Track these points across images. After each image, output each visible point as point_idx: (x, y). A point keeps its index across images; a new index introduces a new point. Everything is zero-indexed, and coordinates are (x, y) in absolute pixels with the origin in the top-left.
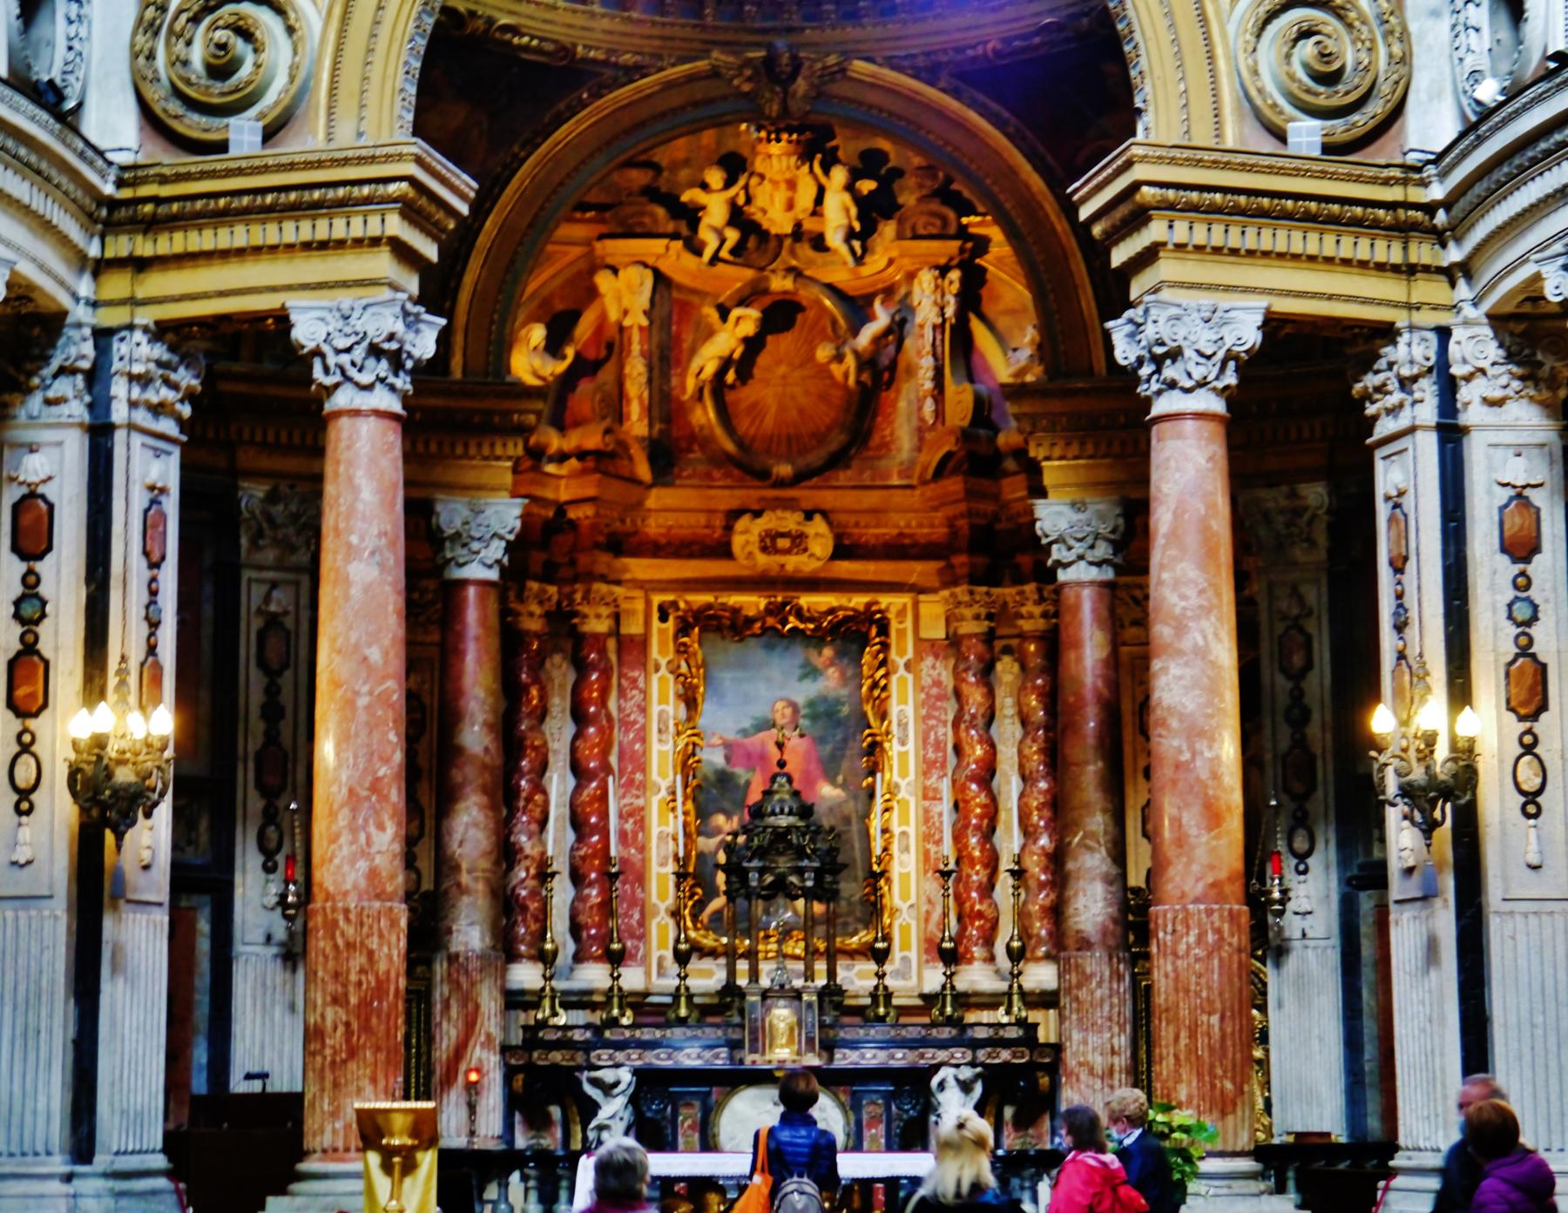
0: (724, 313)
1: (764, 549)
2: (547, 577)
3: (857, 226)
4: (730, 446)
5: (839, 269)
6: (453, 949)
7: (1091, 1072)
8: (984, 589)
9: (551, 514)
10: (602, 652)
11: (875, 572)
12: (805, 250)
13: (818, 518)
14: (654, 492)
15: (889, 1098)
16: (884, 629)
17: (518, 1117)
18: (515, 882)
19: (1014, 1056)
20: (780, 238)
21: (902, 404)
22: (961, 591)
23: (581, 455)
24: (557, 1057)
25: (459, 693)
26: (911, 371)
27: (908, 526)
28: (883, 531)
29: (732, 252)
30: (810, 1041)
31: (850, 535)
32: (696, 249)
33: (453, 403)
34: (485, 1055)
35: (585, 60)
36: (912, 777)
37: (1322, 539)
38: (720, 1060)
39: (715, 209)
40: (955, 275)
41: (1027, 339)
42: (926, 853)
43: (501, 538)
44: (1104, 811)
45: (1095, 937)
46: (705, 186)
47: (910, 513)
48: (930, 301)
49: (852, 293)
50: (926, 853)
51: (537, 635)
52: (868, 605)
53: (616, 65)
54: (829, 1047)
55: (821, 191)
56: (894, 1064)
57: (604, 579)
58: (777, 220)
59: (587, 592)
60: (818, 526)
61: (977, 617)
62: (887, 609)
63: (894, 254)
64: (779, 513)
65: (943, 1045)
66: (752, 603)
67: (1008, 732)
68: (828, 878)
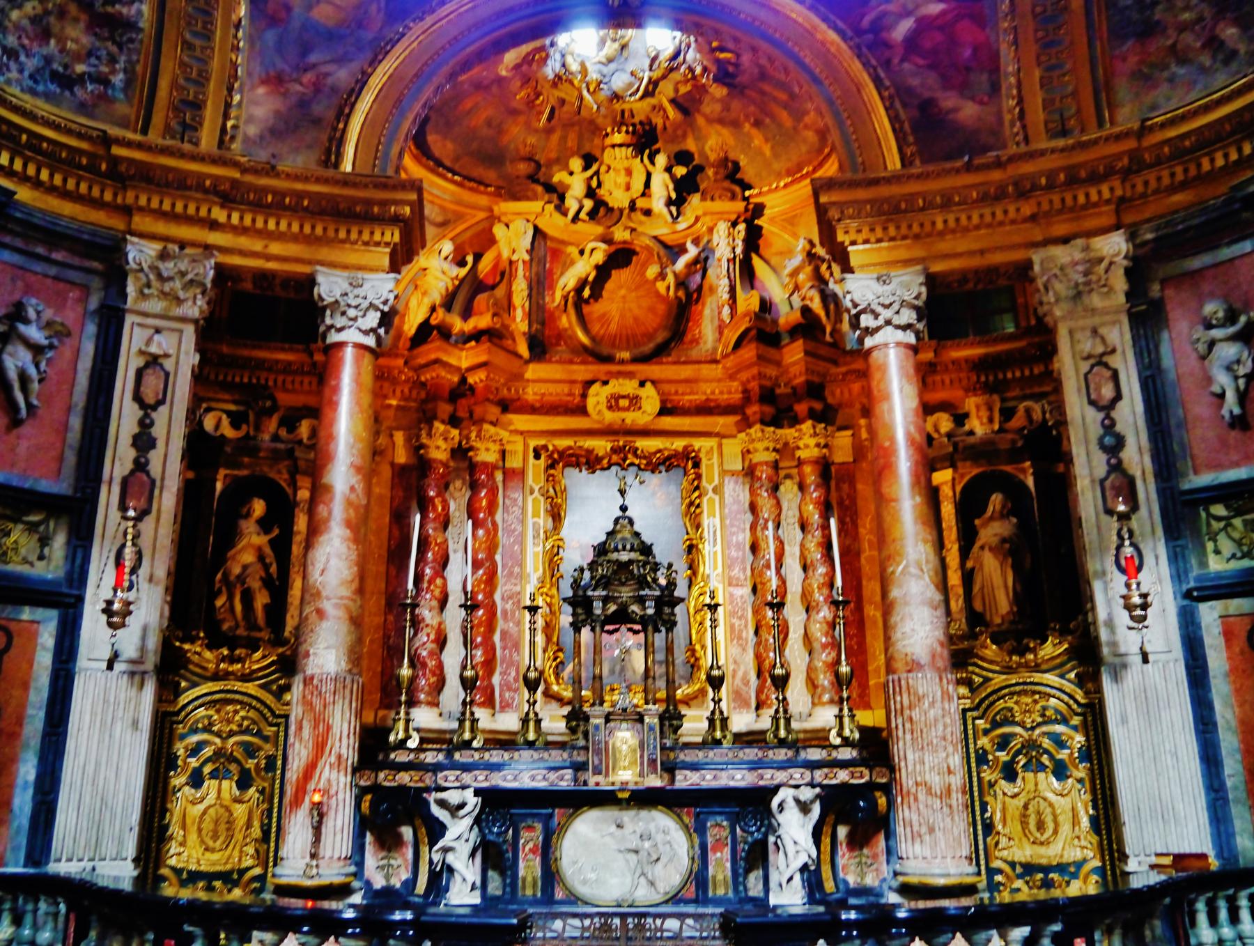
0: (582, 252)
1: (610, 408)
2: (454, 421)
3: (674, 196)
5: (661, 226)
6: (309, 672)
7: (929, 791)
8: (772, 429)
9: (456, 379)
10: (491, 476)
11: (690, 425)
12: (638, 216)
13: (648, 385)
14: (531, 366)
15: (734, 820)
16: (697, 465)
17: (369, 838)
18: (417, 645)
19: (852, 775)
20: (621, 211)
21: (707, 312)
22: (755, 431)
23: (477, 336)
24: (405, 778)
25: (331, 437)
26: (712, 290)
27: (713, 393)
28: (696, 397)
29: (588, 214)
30: (652, 762)
31: (671, 401)
32: (561, 209)
33: (336, 191)
34: (334, 775)
36: (720, 569)
37: (1120, 284)
38: (565, 781)
40: (742, 227)
41: (800, 247)
42: (732, 626)
43: (377, 309)
44: (925, 541)
45: (924, 657)
46: (571, 173)
47: (715, 383)
48: (725, 244)
49: (670, 243)
50: (732, 626)
51: (446, 465)
52: (685, 448)
54: (670, 769)
55: (649, 175)
56: (732, 784)
57: (494, 424)
58: (617, 197)
59: (480, 431)
60: (649, 390)
61: (767, 449)
62: (699, 450)
63: (700, 213)
64: (621, 381)
65: (782, 766)
66: (601, 446)
67: (792, 534)
68: (667, 610)
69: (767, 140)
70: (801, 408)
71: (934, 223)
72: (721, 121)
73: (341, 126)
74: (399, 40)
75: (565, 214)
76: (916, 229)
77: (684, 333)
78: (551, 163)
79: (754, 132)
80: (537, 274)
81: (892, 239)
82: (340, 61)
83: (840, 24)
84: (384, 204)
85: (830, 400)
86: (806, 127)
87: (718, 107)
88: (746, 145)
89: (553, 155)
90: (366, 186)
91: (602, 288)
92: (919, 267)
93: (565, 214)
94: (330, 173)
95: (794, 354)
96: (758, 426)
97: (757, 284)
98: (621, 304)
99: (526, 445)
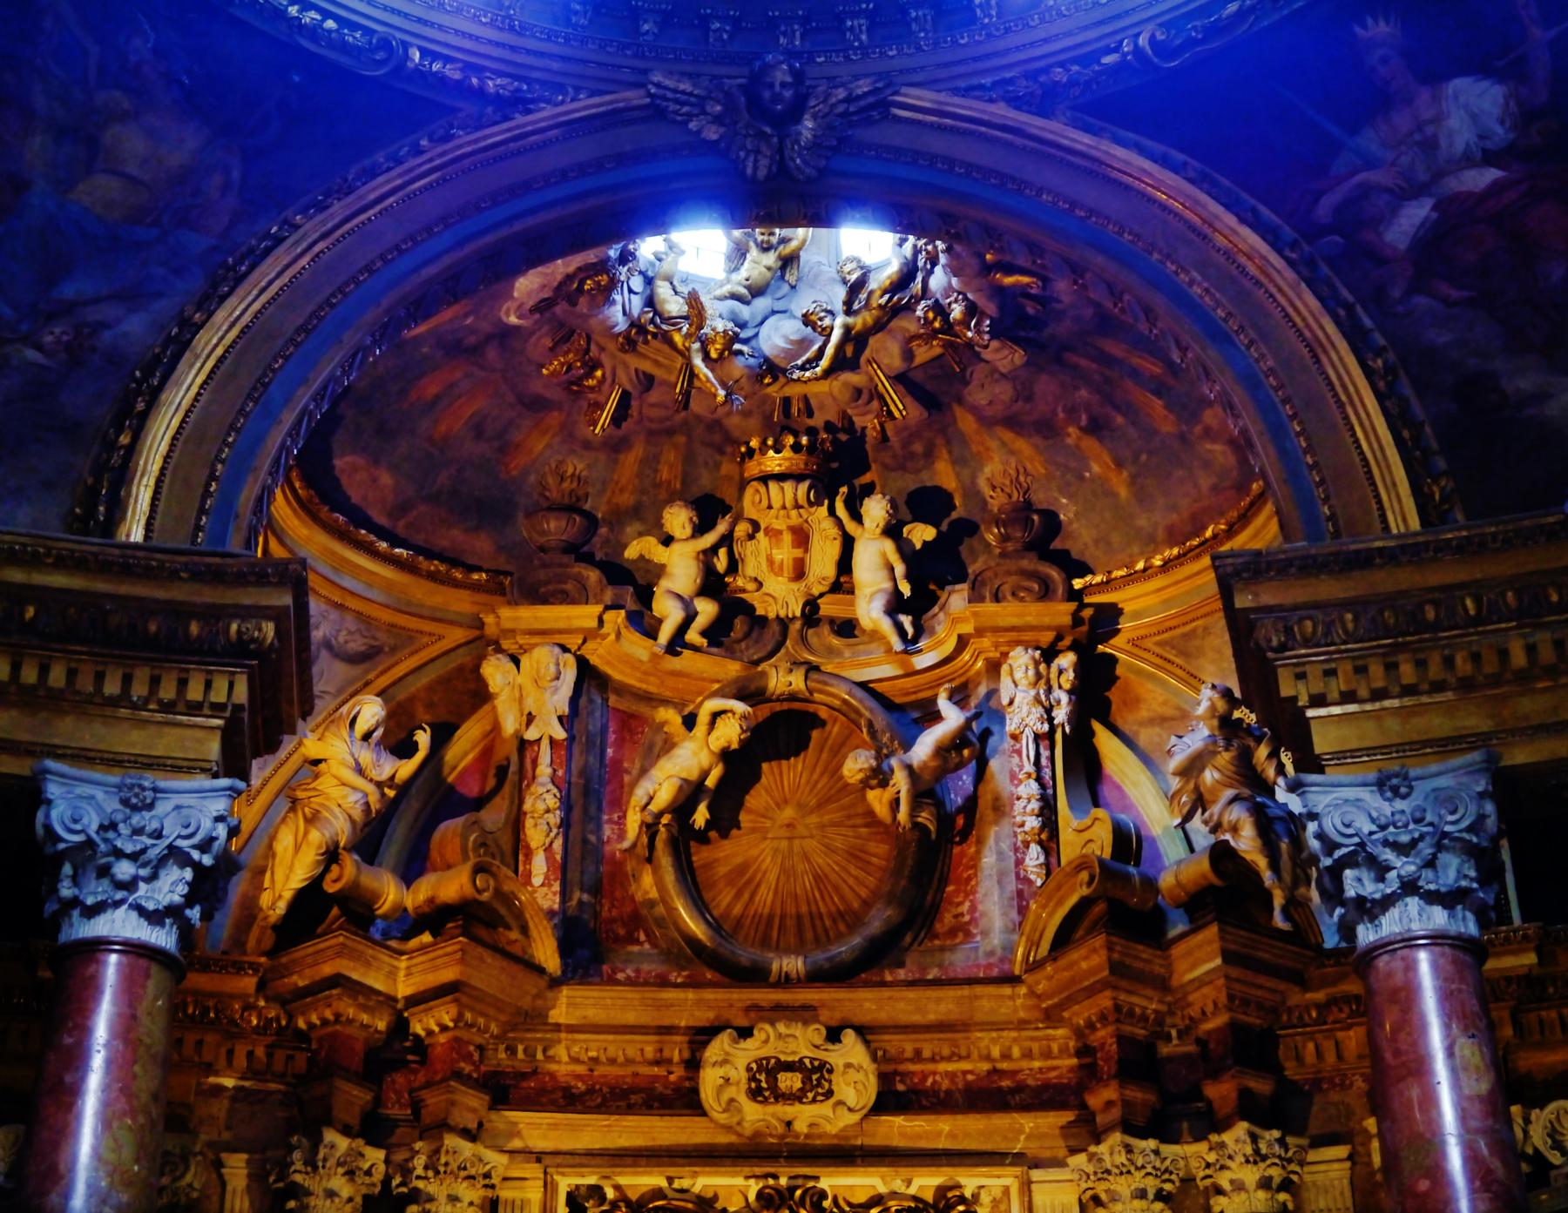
0: (690, 722)
1: (755, 1094)
2: (373, 1129)
4: (695, 926)
8: (1152, 1144)
11: (952, 1135)
13: (849, 1036)
14: (565, 991)
21: (988, 860)
22: (1110, 1149)
23: (436, 919)
26: (1000, 808)
27: (1006, 1056)
28: (965, 1066)
29: (704, 633)
31: (905, 1075)
32: (645, 624)
35: (420, 74)
39: (680, 569)
40: (1067, 660)
41: (1201, 710)
43: (184, 860)
48: (1027, 699)
49: (898, 700)
52: (941, 1191)
53: (481, 93)
55: (848, 544)
57: (471, 1136)
58: (779, 597)
61: (1141, 1194)
62: (976, 1196)
63: (967, 628)
69: (1119, 464)
70: (1220, 1091)
71: (1504, 654)
72: (1012, 422)
73: (124, 439)
74: (267, 252)
75: (652, 634)
76: (1463, 665)
77: (934, 911)
78: (619, 517)
79: (1090, 444)
80: (584, 773)
81: (1408, 691)
82: (133, 297)
83: (1265, 211)
84: (215, 615)
85: (1291, 1071)
86: (1208, 434)
87: (1004, 391)
88: (1072, 475)
89: (626, 499)
90: (174, 575)
91: (739, 805)
92: (1476, 756)
93: (652, 634)
94: (92, 544)
95: (1199, 960)
96: (1116, 1138)
97: (1106, 792)
98: (784, 844)
99: (549, 1187)
